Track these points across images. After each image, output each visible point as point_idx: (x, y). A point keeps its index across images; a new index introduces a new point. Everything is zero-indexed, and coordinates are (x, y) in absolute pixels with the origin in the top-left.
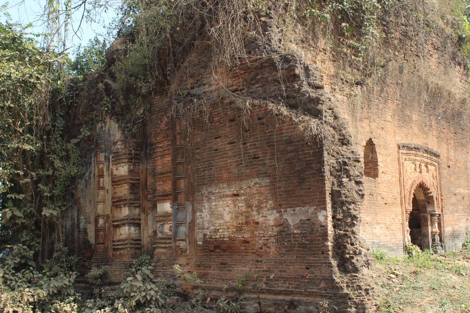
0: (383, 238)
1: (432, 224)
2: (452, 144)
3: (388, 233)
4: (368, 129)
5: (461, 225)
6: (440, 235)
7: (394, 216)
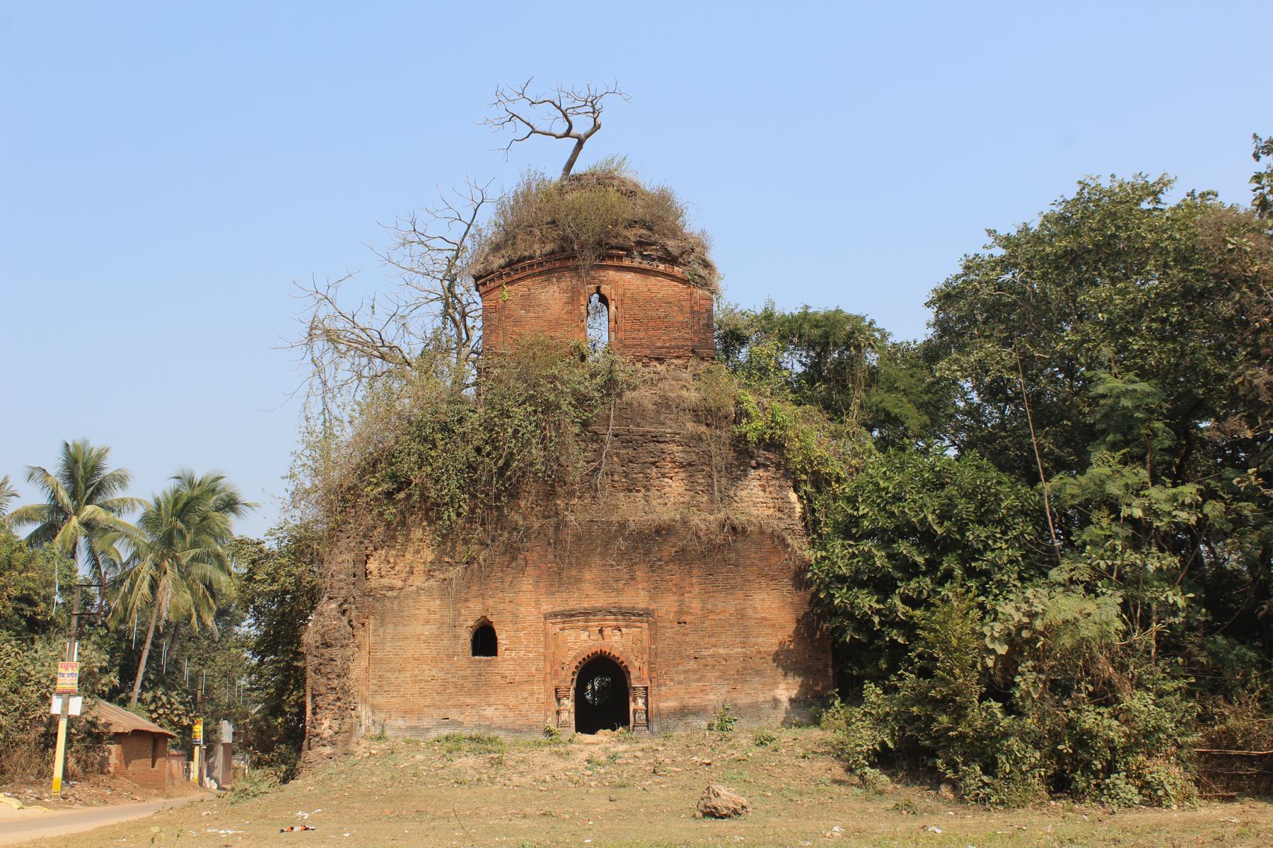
0: (498, 720)
1: (635, 700)
2: (696, 590)
3: (510, 714)
4: (480, 607)
5: (711, 697)
6: (647, 712)
7: (525, 695)
